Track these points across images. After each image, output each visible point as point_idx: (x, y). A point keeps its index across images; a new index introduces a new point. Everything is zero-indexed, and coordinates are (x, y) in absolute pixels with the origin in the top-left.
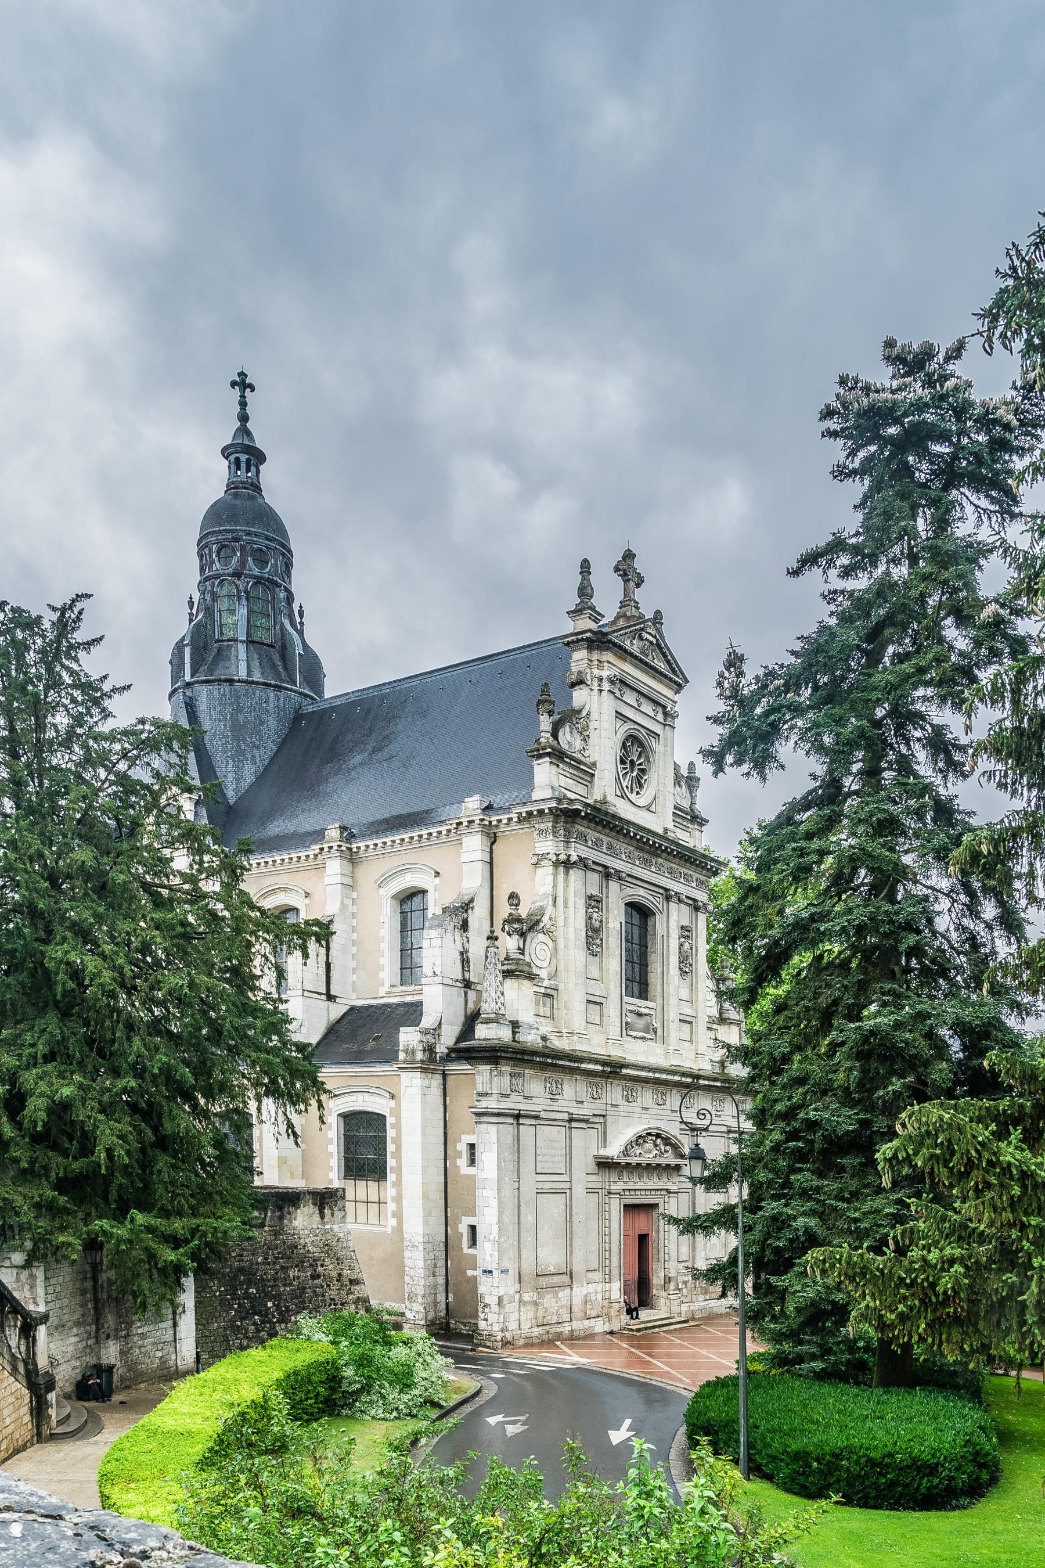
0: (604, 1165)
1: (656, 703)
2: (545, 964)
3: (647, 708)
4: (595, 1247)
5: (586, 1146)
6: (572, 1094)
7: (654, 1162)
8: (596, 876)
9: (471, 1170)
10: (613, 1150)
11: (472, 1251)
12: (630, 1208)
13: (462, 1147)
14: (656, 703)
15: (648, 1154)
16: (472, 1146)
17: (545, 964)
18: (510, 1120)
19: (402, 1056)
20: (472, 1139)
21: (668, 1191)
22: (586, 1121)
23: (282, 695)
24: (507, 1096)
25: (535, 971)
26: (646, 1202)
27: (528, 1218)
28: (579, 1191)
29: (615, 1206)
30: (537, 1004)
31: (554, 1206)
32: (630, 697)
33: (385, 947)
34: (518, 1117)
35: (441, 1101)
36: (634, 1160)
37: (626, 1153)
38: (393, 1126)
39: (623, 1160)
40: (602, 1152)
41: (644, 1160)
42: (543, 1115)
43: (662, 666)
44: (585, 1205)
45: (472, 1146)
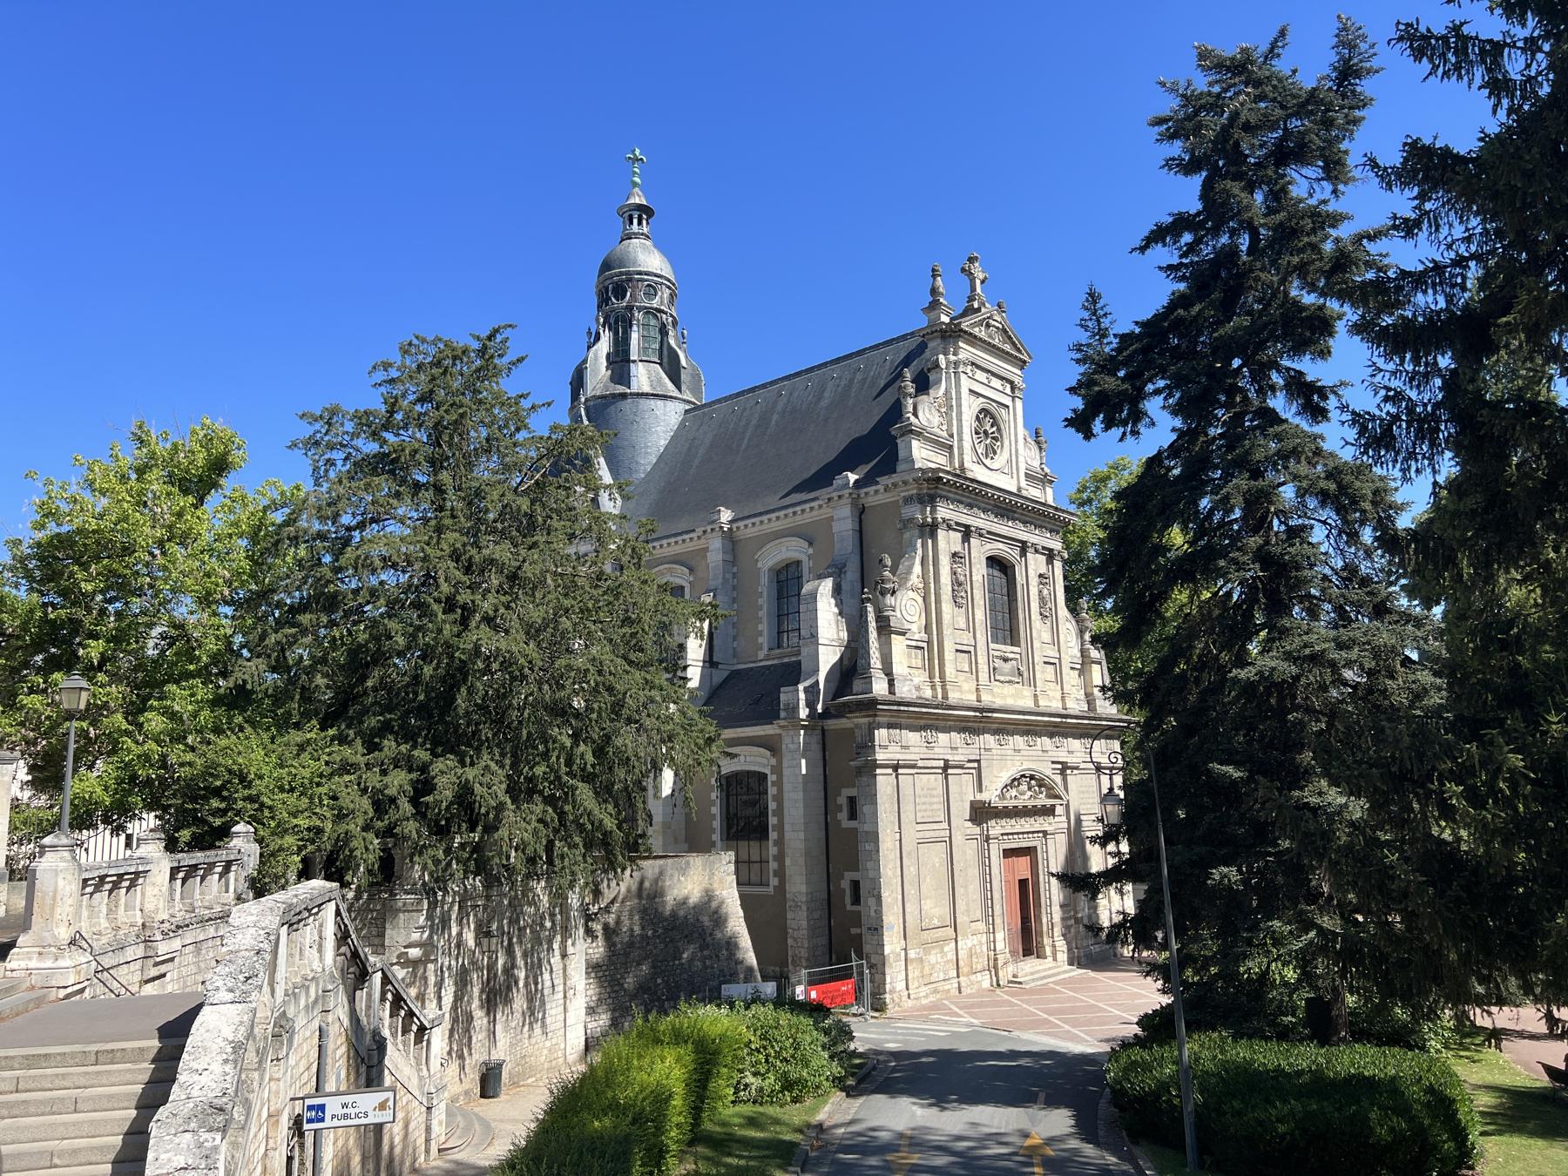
0: (981, 813)
1: (1002, 378)
2: (915, 619)
3: (996, 383)
4: (977, 896)
5: (964, 791)
6: (947, 744)
7: (1030, 804)
8: (959, 535)
9: (853, 824)
10: (991, 795)
11: (855, 908)
12: (1009, 853)
13: (842, 800)
14: (1002, 378)
15: (1025, 797)
16: (852, 801)
17: (915, 619)
18: (890, 771)
19: (783, 714)
20: (852, 792)
21: (1045, 833)
22: (962, 767)
23: (670, 405)
24: (886, 747)
25: (907, 626)
26: (1024, 845)
27: (910, 871)
28: (958, 839)
29: (995, 851)
30: (909, 656)
31: (937, 854)
32: (980, 376)
33: (763, 613)
34: (896, 768)
35: (820, 755)
36: (1010, 803)
37: (1002, 796)
38: (773, 783)
39: (1000, 805)
40: (979, 797)
41: (1019, 803)
42: (920, 763)
43: (1007, 347)
44: (967, 852)
45: (852, 801)
